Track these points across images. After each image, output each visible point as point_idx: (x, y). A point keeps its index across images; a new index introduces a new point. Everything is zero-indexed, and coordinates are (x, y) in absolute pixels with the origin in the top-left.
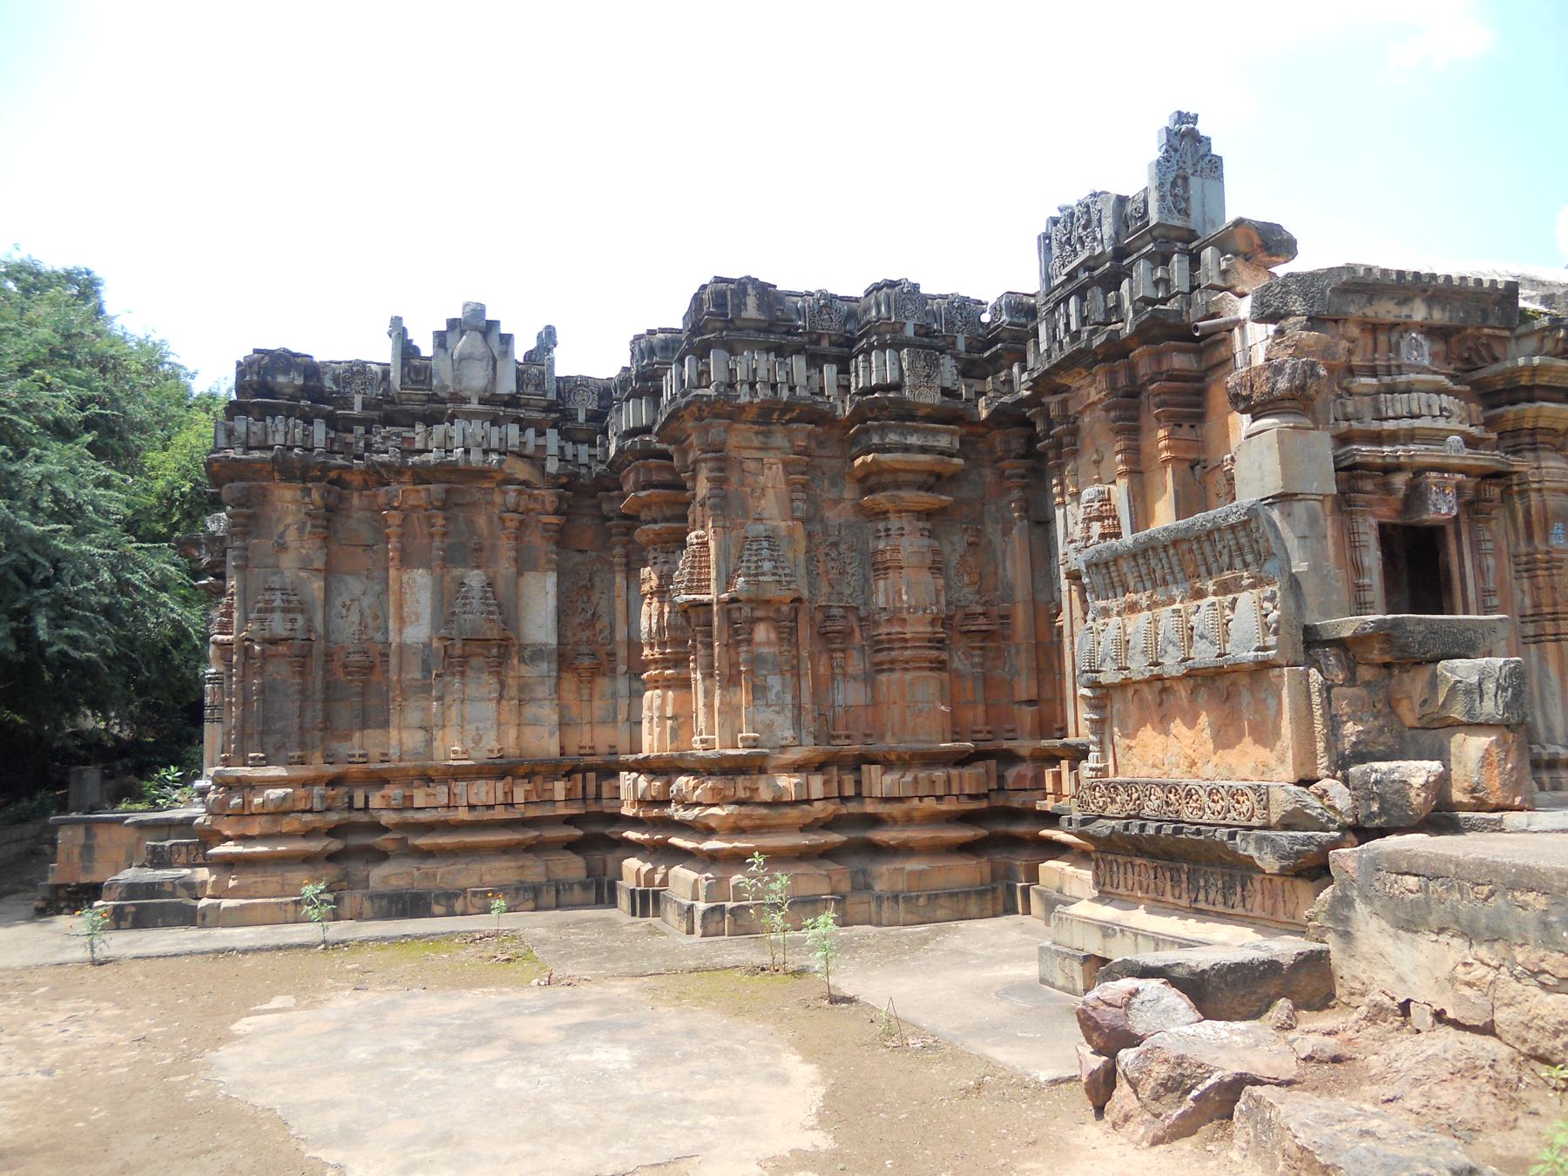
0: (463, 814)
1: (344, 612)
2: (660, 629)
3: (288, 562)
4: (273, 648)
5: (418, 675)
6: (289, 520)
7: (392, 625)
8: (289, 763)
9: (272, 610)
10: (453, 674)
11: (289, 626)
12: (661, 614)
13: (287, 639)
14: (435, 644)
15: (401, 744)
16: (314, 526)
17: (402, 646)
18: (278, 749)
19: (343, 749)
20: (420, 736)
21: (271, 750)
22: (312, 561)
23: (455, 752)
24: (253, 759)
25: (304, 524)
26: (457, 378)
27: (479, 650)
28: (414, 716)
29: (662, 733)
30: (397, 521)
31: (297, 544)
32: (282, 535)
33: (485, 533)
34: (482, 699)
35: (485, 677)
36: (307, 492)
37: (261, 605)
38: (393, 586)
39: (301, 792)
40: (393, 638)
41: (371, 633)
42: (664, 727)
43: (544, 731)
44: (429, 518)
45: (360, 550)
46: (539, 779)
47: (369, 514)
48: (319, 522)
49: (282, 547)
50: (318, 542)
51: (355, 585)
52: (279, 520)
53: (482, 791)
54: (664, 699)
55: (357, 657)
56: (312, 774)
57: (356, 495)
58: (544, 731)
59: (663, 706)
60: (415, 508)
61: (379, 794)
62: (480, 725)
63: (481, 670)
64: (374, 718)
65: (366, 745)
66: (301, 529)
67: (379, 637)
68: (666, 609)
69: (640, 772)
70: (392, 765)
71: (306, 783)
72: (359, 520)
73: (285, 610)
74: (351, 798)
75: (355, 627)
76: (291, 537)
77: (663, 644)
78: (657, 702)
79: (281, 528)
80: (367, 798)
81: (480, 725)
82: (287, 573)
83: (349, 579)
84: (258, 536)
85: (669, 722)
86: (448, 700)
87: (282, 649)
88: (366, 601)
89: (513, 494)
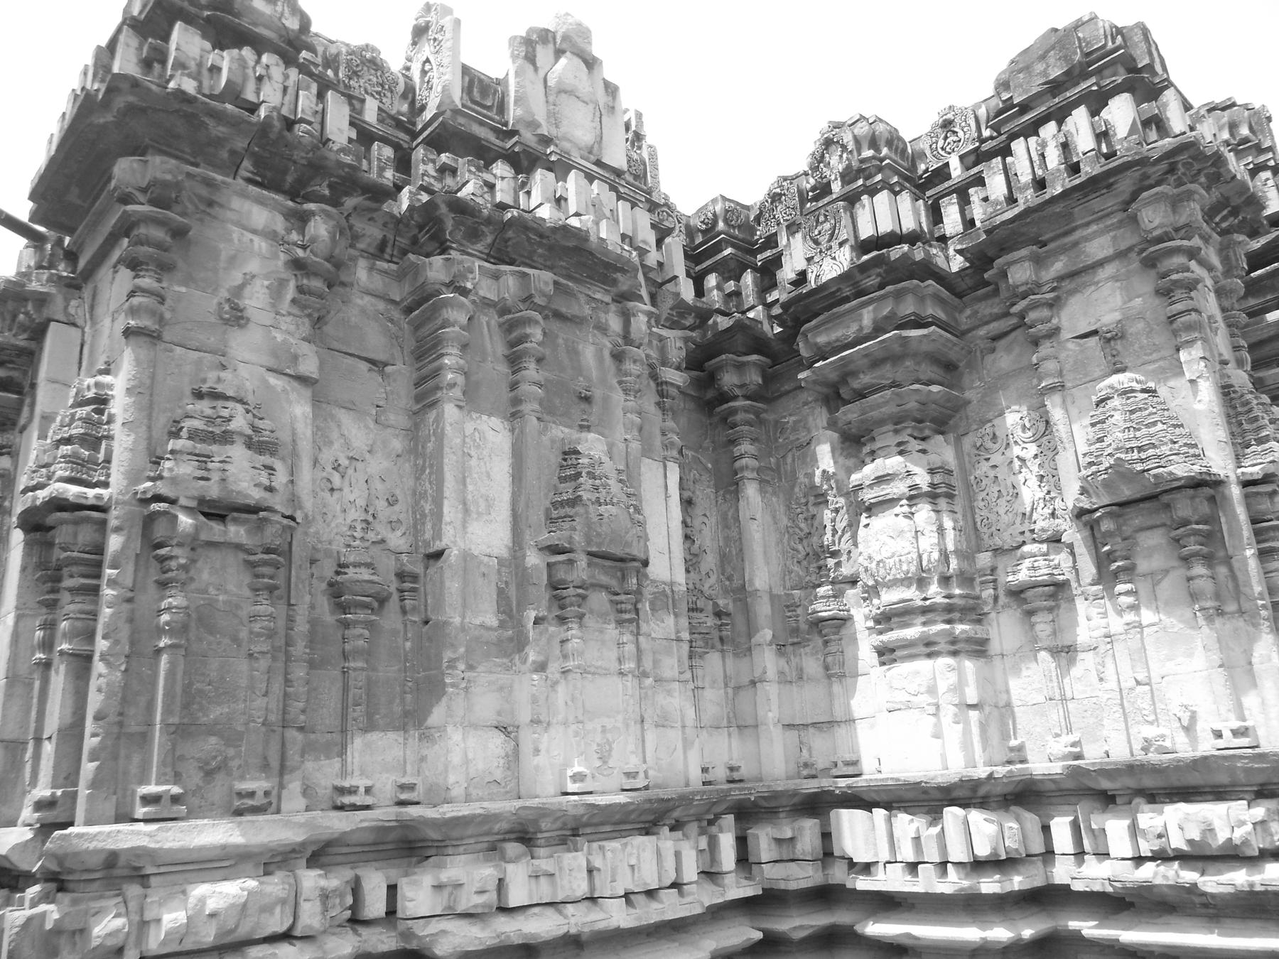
0: (618, 916)
1: (336, 478)
2: (945, 556)
3: (248, 349)
4: (216, 526)
5: (492, 621)
6: (253, 266)
7: (450, 511)
8: (241, 808)
9: (226, 438)
10: (562, 620)
11: (264, 478)
12: (941, 530)
13: (253, 510)
14: (534, 559)
15: (466, 761)
16: (300, 290)
17: (467, 556)
18: (209, 774)
19: (325, 773)
20: (497, 743)
21: (196, 778)
22: (295, 358)
23: (578, 777)
24: (148, 800)
25: (282, 283)
26: (554, 117)
27: (604, 579)
28: (486, 704)
29: (967, 732)
30: (463, 319)
31: (267, 318)
32: (239, 290)
33: (594, 374)
34: (607, 673)
35: (611, 631)
36: (301, 220)
37: (198, 424)
38: (452, 438)
39: (276, 885)
40: (450, 538)
41: (382, 530)
42: (967, 723)
43: (674, 736)
44: (509, 327)
45: (364, 366)
46: (693, 828)
47: (381, 306)
48: (317, 284)
49: (236, 317)
50: (306, 328)
51: (355, 432)
52: (232, 260)
53: (641, 859)
54: (960, 672)
55: (365, 574)
56: (294, 836)
57: (362, 264)
58: (674, 736)
59: (959, 688)
60: (486, 303)
61: (426, 878)
62: (609, 722)
63: (603, 616)
64: (412, 703)
65: (376, 764)
66: (276, 291)
67: (397, 540)
68: (948, 523)
69: (965, 804)
70: (448, 811)
71: (272, 861)
72: (363, 311)
73: (249, 444)
74: (356, 888)
75: (355, 515)
76: (256, 300)
77: (945, 580)
78: (953, 678)
79: (236, 278)
80: (392, 889)
81: (609, 722)
82: (243, 371)
83: (344, 417)
84: (188, 280)
85: (974, 715)
86: (554, 668)
87: (236, 532)
88: (377, 465)
89: (643, 318)
